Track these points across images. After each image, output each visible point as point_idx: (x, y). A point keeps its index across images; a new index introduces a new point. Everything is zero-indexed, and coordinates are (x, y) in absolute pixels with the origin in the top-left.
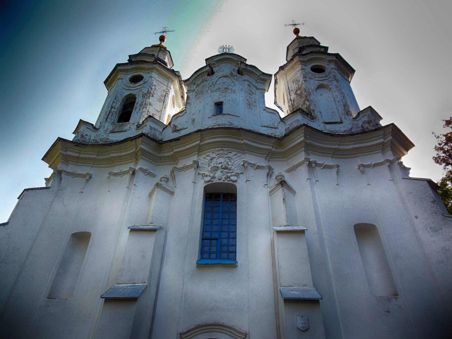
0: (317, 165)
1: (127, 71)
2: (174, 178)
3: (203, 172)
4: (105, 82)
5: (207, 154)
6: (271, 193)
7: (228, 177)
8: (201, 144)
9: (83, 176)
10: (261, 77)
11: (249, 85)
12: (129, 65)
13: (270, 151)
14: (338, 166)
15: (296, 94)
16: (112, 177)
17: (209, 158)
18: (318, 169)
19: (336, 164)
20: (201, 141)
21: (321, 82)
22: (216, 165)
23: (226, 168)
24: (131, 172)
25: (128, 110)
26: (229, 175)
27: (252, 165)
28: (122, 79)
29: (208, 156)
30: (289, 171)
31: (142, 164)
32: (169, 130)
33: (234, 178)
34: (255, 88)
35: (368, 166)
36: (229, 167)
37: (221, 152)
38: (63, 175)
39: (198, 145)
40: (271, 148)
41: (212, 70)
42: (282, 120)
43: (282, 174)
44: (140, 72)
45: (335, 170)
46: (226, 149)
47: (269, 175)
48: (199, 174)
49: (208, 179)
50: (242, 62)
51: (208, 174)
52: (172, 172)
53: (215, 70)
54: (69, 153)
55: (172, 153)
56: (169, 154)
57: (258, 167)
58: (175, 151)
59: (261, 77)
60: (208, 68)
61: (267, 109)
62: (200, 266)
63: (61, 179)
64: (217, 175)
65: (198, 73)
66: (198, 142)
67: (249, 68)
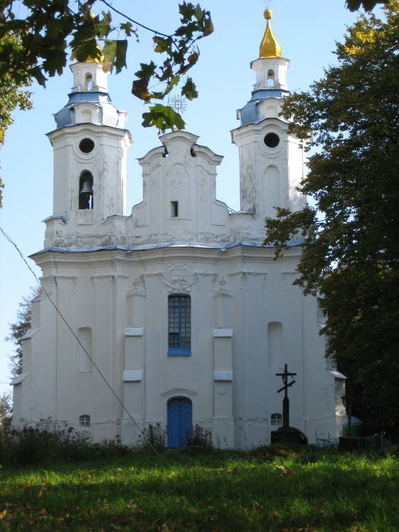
0: (249, 273)
1: (75, 133)
2: (143, 282)
3: (166, 283)
4: (48, 135)
5: (169, 265)
6: (215, 297)
7: (184, 289)
8: (164, 256)
9: (74, 278)
10: (214, 159)
11: (201, 172)
12: (76, 127)
13: (216, 259)
14: (266, 274)
15: (248, 169)
16: (95, 280)
17: (170, 269)
18: (250, 277)
19: (264, 272)
20: (163, 254)
21: (272, 162)
22: (176, 278)
23: (183, 280)
24: (111, 279)
25: (85, 190)
26: (185, 286)
27: (202, 274)
28: (72, 146)
29: (168, 267)
30: (229, 275)
31: (119, 271)
32: (131, 223)
33: (188, 289)
34: (207, 174)
35: (289, 273)
36: (185, 279)
37: (178, 265)
38: (58, 281)
39: (162, 258)
40: (216, 256)
41: (166, 151)
42: (230, 215)
43: (225, 279)
44: (88, 133)
45: (263, 277)
46: (182, 261)
47: (214, 280)
48: (163, 283)
49: (170, 290)
50: (195, 144)
51: (170, 285)
52: (142, 277)
53: (168, 150)
54: (57, 260)
55: (139, 259)
56: (137, 259)
57: (207, 275)
58: (143, 258)
59: (214, 159)
60: (162, 150)
61: (219, 204)
62: (170, 355)
63: (56, 283)
64: (176, 287)
65: (153, 153)
66: (160, 256)
67: (202, 150)
